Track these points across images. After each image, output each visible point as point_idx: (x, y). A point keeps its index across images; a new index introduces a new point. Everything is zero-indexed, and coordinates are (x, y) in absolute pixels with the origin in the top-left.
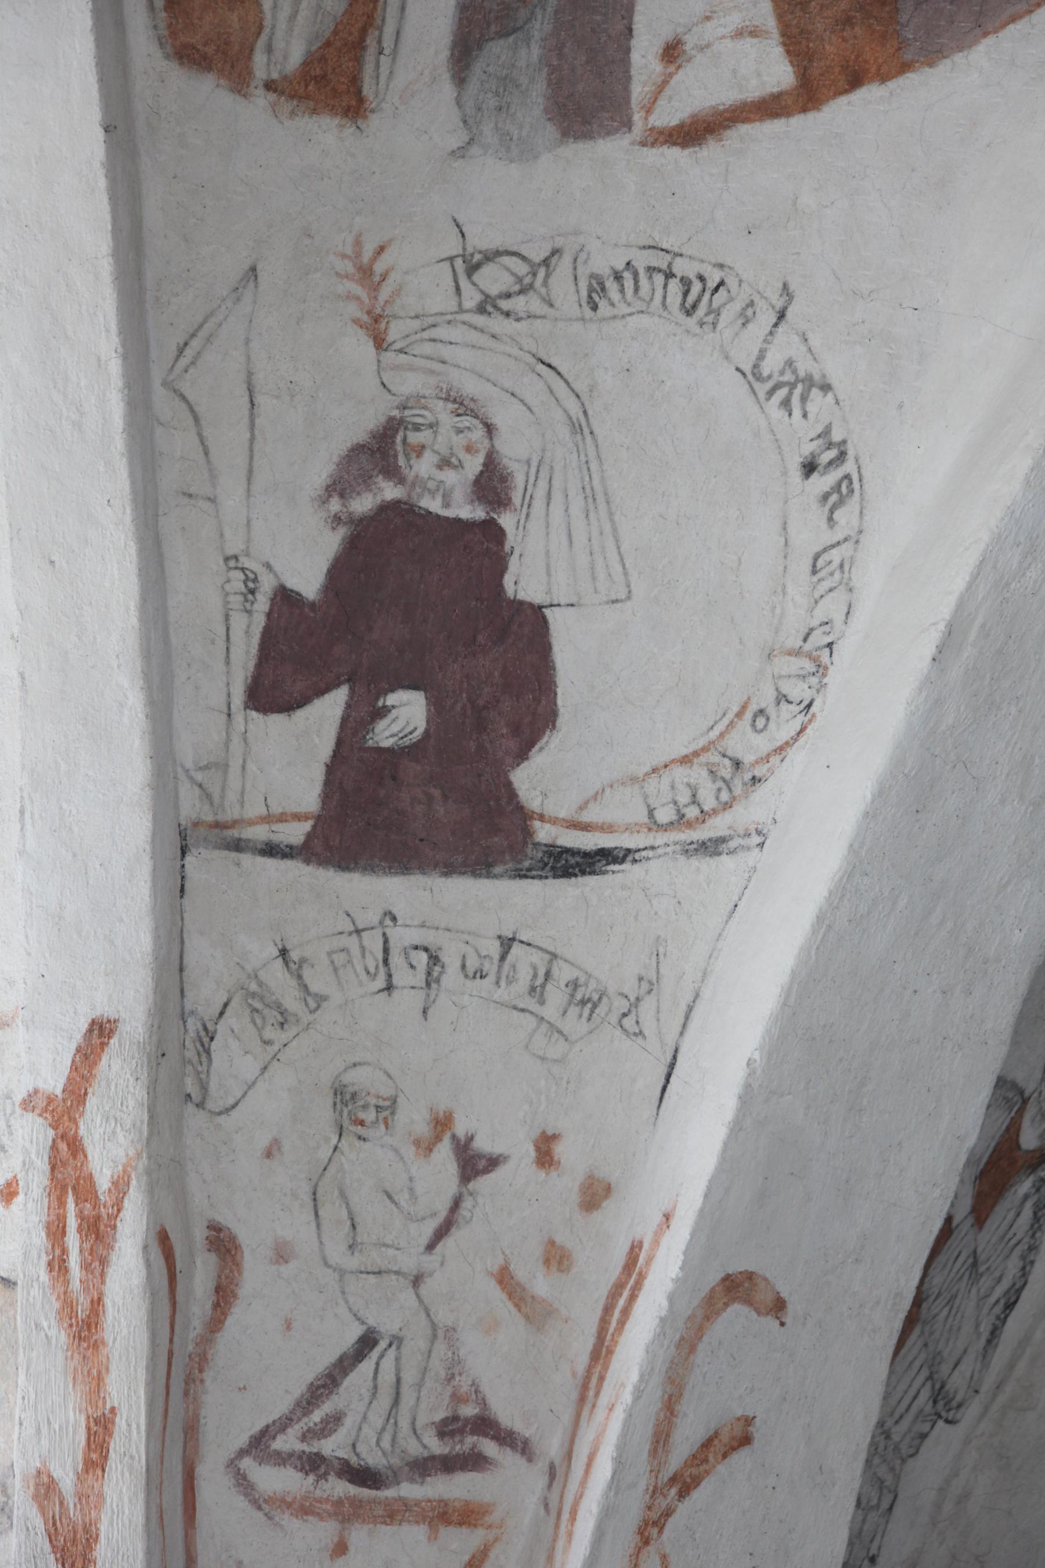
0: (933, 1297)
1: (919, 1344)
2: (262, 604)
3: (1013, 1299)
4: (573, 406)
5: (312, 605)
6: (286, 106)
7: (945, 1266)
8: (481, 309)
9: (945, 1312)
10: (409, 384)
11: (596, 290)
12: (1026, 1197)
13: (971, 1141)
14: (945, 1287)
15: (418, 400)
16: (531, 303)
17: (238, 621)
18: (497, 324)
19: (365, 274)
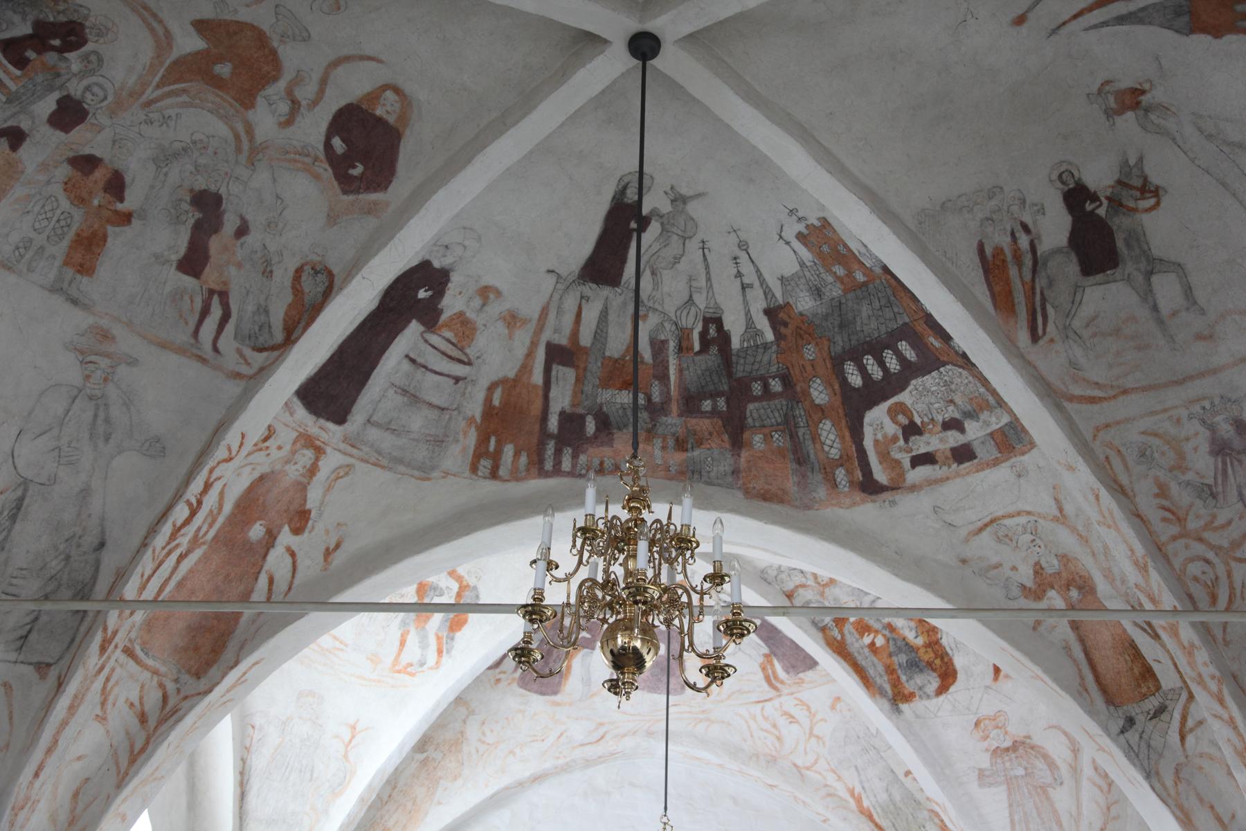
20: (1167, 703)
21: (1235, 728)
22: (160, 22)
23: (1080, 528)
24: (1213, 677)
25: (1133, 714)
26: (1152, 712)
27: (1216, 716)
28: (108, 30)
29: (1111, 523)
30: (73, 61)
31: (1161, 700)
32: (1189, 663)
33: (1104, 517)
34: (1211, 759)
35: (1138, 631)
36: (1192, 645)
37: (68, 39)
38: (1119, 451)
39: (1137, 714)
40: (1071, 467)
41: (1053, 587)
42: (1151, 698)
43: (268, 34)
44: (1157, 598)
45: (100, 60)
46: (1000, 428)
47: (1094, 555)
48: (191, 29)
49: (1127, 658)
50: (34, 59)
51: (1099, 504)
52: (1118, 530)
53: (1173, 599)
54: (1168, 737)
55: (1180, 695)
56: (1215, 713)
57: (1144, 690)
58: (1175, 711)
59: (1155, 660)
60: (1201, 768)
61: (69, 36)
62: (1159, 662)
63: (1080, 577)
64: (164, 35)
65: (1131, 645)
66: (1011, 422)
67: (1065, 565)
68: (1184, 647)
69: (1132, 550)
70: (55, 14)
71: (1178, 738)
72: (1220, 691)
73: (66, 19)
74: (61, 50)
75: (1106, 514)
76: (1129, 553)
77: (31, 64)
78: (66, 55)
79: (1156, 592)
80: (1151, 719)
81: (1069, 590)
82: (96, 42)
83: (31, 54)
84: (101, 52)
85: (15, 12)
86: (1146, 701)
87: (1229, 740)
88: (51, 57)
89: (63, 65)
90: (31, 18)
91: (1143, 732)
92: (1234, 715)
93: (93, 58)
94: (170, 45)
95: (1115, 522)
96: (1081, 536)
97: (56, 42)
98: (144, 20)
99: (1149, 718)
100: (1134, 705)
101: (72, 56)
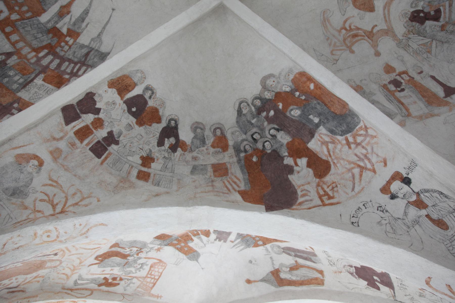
0: (439, 216)
1: (446, 218)
2: (369, 287)
3: (441, 193)
4: (340, 260)
5: (368, 282)
6: (324, 277)
7: (433, 214)
8: (335, 265)
9: (441, 212)
10: (344, 271)
11: (329, 256)
12: (424, 195)
13: (403, 250)
14: (437, 213)
15: (345, 270)
16: (332, 261)
17: (372, 290)
18: (335, 263)
19: (336, 272)
22: (384, 14)
28: (402, 15)
30: (421, 6)
37: (417, 15)
43: (351, 3)
45: (412, 4)
48: (376, 9)
50: (433, 11)
61: (416, 16)
64: (386, 8)
70: (415, 26)
73: (413, 23)
74: (422, 11)
77: (435, 10)
78: (422, 9)
82: (409, 11)
83: (432, 13)
84: (410, 7)
85: (426, 31)
88: (426, 10)
89: (425, 6)
90: (423, 27)
93: (414, 5)
94: (386, 4)
97: (422, 15)
98: (389, 15)
101: (420, 8)
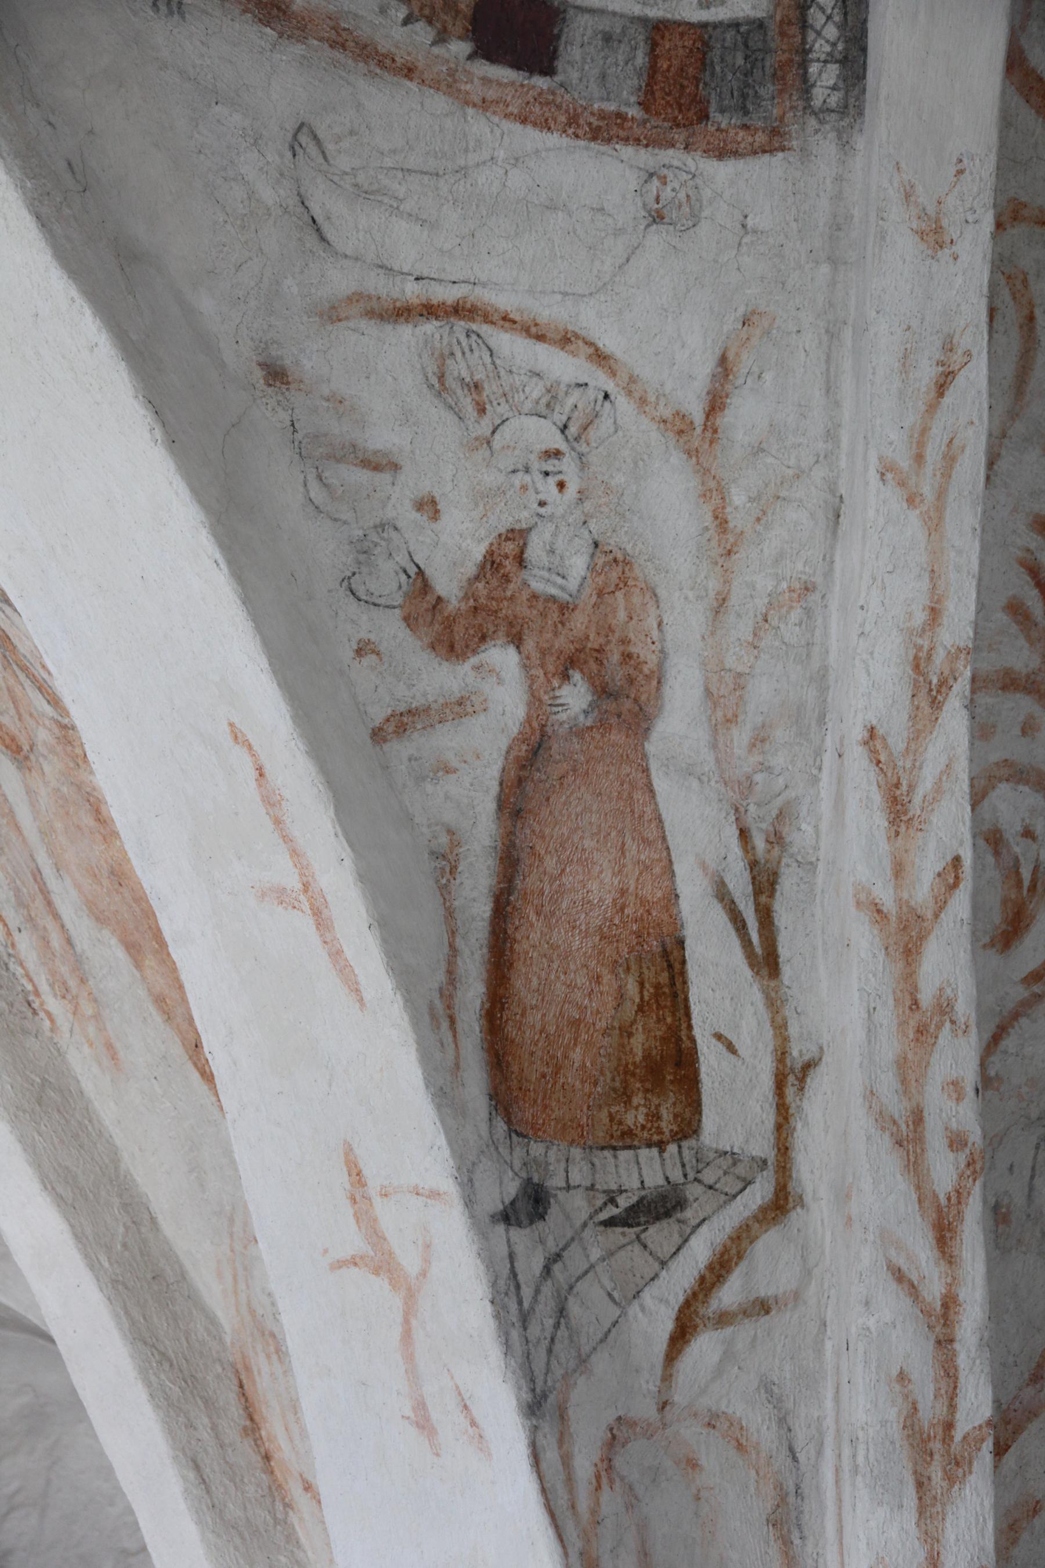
20: (693, 1191)
21: (945, 1343)
23: (738, 497)
24: (956, 1142)
25: (557, 1181)
26: (624, 1202)
27: (899, 1276)
29: (927, 490)
31: (676, 1176)
32: (902, 1064)
33: (919, 458)
34: (740, 1447)
35: (719, 916)
36: (944, 1008)
38: (1031, 318)
39: (568, 1188)
40: (938, 230)
41: (517, 640)
42: (644, 1153)
44: (915, 809)
46: (704, 25)
47: (721, 605)
49: (632, 988)
51: (932, 408)
52: (934, 524)
53: (968, 837)
54: (634, 1309)
55: (747, 1183)
56: (901, 1262)
57: (635, 1117)
58: (704, 1229)
59: (719, 1037)
60: (693, 1464)
62: (731, 1048)
63: (627, 657)
65: (665, 954)
66: (760, 25)
67: (600, 594)
68: (915, 1004)
69: (935, 613)
71: (666, 1325)
72: (959, 1195)
75: (933, 453)
76: (920, 617)
79: (925, 785)
80: (610, 1223)
81: (566, 677)
86: (624, 1155)
87: (902, 1377)
91: (558, 1257)
92: (963, 1294)
95: (941, 494)
96: (722, 523)
99: (604, 1216)
100: (576, 1152)
